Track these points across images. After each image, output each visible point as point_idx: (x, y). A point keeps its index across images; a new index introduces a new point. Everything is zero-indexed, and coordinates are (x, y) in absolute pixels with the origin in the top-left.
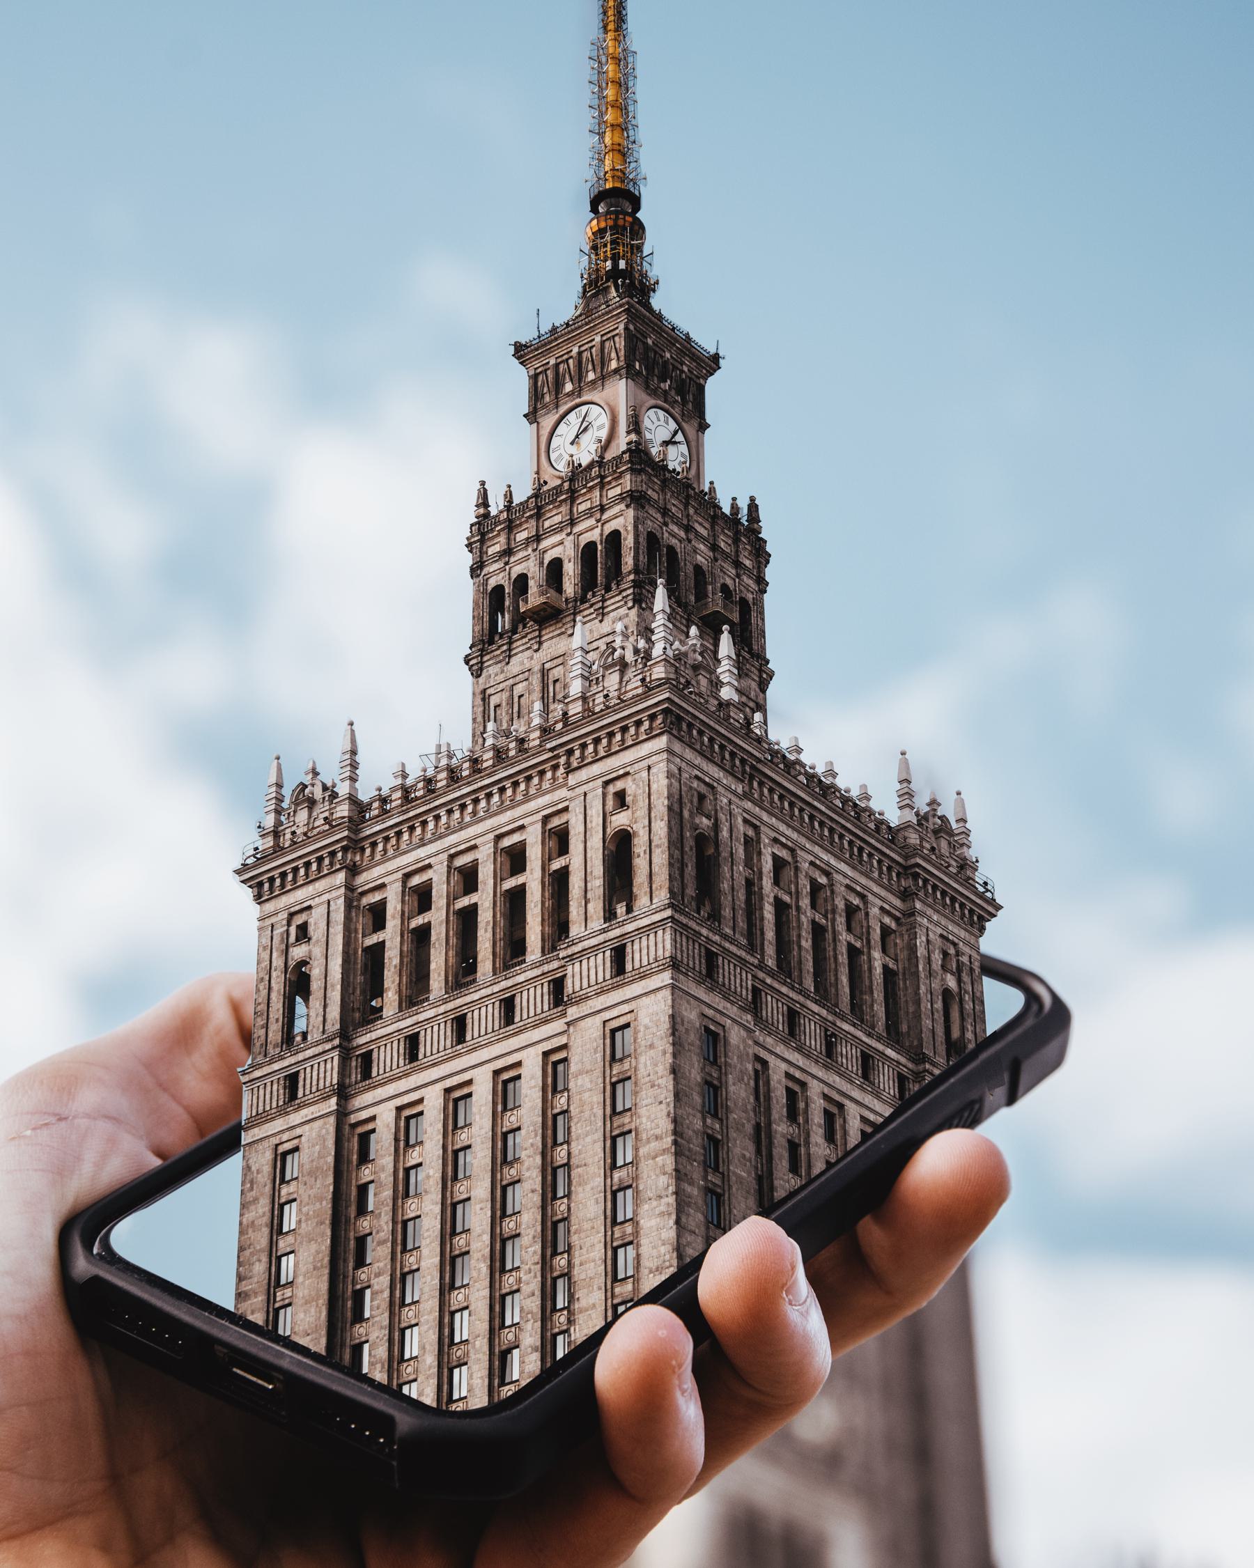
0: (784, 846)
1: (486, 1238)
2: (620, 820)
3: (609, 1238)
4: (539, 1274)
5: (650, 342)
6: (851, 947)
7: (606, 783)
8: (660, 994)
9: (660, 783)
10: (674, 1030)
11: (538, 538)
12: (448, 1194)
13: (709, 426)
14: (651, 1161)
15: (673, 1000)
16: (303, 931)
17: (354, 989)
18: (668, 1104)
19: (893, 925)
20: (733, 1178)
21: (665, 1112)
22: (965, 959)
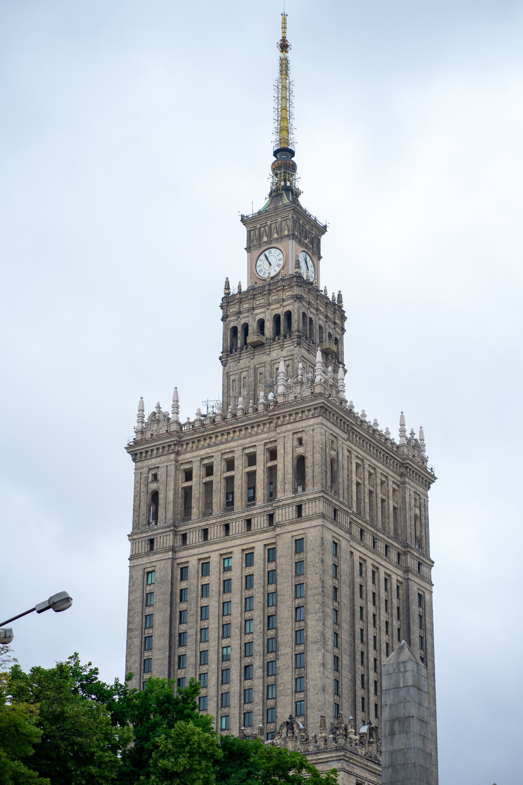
0: (359, 458)
1: (239, 619)
2: (300, 450)
3: (293, 627)
4: (262, 637)
5: (301, 222)
6: (383, 500)
7: (294, 433)
8: (317, 528)
9: (318, 437)
10: (322, 544)
11: (254, 309)
12: (221, 598)
13: (322, 257)
14: (312, 598)
16: (155, 476)
17: (178, 505)
18: (320, 575)
19: (396, 488)
20: (342, 604)
21: (319, 578)
22: (422, 501)
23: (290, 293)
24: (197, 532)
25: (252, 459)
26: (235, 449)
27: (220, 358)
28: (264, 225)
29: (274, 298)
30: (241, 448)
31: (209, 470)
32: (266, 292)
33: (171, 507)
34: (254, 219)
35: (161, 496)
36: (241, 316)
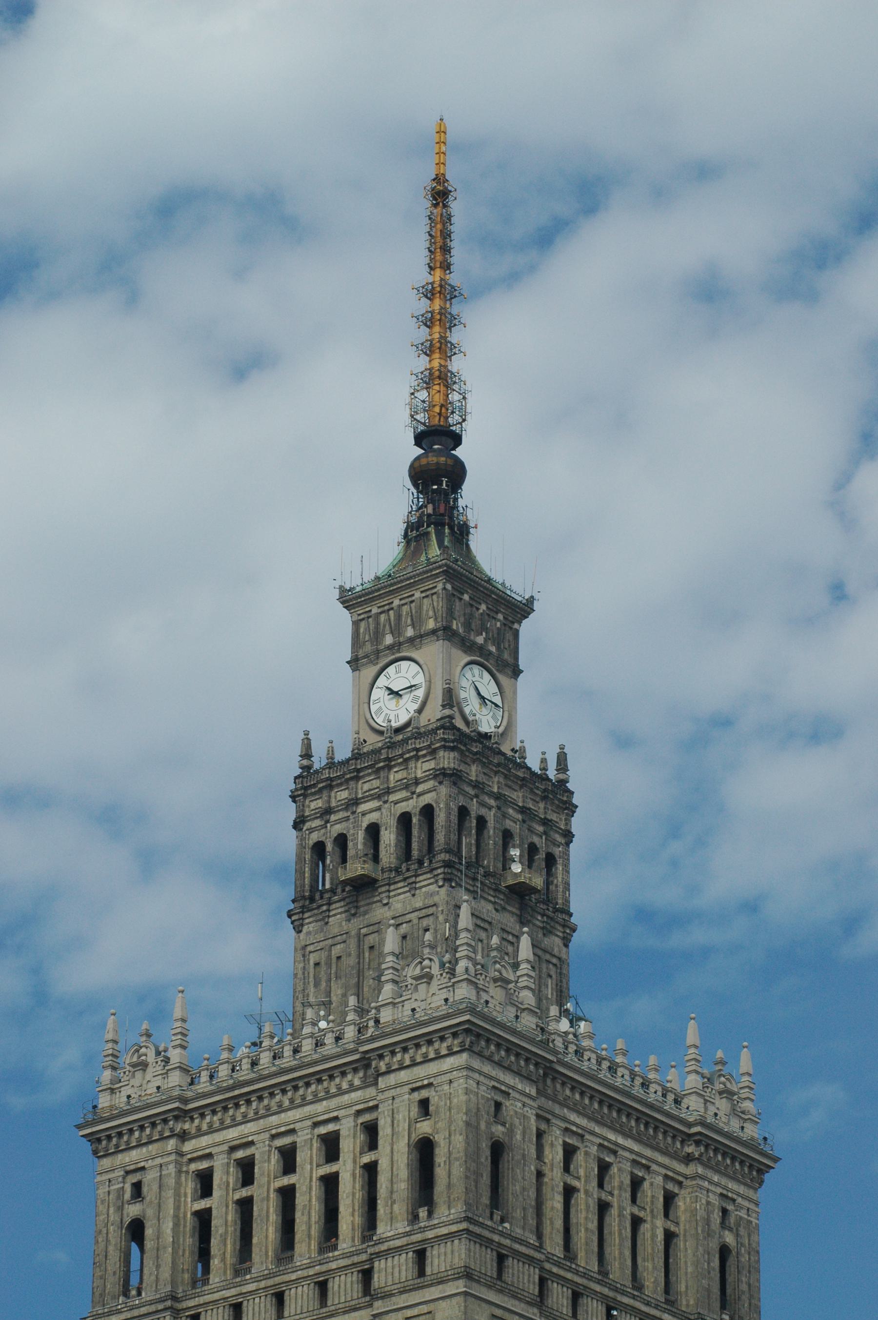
2: (425, 1127)
7: (413, 1090)
8: (455, 1300)
9: (460, 1099)
15: (466, 1307)
16: (137, 1187)
17: (184, 1250)
23: (432, 765)
24: (221, 1310)
25: (331, 1147)
26: (297, 1126)
27: (290, 915)
28: (386, 608)
29: (399, 776)
30: (309, 1123)
31: (247, 1171)
32: (382, 764)
33: (167, 1256)
34: (367, 594)
35: (149, 1232)
36: (333, 818)
